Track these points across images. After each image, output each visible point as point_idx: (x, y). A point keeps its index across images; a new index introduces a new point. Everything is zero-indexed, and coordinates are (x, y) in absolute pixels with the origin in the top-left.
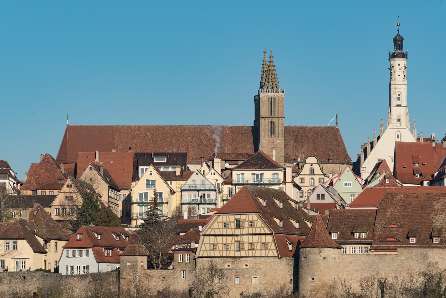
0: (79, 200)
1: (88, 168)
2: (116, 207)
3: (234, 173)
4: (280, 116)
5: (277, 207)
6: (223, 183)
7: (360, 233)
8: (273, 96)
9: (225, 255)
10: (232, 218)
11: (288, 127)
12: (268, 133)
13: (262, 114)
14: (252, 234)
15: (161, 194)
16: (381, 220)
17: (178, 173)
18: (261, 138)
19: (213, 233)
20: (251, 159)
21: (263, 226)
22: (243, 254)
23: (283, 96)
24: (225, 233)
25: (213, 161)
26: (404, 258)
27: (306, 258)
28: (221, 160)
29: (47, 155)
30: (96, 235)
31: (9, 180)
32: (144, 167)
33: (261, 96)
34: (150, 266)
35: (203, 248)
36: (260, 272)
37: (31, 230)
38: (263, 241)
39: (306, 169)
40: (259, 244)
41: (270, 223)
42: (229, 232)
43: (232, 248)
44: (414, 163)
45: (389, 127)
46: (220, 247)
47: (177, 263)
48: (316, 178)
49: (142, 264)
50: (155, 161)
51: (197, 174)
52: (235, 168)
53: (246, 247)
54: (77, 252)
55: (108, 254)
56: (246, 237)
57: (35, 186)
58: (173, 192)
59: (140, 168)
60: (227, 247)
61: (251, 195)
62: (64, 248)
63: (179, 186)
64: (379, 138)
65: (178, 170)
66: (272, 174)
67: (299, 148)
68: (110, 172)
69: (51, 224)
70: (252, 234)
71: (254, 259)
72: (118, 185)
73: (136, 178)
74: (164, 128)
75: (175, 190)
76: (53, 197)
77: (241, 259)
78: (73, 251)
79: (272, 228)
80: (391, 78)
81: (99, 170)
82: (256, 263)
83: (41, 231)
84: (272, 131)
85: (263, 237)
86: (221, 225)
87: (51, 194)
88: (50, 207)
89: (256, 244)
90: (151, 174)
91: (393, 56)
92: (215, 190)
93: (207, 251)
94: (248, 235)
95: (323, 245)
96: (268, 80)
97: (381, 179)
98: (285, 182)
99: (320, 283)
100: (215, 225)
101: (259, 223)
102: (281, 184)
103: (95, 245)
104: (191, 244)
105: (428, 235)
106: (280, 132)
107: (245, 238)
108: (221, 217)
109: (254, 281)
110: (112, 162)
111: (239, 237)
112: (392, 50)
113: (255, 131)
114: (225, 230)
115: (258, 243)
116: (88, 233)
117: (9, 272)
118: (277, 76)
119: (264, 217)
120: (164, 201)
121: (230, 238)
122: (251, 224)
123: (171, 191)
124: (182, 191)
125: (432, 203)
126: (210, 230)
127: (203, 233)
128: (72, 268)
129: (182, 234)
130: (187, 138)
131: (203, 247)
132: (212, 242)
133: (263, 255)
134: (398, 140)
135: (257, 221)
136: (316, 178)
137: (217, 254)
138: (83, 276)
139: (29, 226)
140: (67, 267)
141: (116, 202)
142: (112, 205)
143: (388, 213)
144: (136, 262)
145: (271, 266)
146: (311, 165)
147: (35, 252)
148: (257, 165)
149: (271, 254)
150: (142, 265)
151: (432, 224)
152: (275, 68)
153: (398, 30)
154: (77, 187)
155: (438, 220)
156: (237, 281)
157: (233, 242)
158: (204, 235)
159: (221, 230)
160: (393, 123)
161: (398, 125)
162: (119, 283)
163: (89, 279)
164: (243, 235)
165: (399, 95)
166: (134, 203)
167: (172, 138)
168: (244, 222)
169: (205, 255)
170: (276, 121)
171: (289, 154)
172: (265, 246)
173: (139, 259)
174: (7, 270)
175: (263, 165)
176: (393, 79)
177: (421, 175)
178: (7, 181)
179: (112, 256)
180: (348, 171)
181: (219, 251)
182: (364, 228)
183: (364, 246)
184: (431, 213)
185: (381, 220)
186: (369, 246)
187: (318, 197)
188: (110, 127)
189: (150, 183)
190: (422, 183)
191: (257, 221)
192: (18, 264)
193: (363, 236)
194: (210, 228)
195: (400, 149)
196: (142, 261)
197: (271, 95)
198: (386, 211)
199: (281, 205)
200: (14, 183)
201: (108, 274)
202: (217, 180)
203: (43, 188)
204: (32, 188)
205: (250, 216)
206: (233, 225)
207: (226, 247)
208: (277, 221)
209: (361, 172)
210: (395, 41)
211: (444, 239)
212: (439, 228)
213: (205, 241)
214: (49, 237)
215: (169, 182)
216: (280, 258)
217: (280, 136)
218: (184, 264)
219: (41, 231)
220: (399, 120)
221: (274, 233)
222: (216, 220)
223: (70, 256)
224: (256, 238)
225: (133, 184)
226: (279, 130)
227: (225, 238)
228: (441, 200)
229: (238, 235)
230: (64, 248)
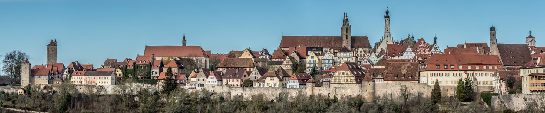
10: (341, 72)
39: (359, 52)
41: (353, 73)
76: (283, 62)
151: (401, 72)
189: (312, 57)
203: (278, 58)
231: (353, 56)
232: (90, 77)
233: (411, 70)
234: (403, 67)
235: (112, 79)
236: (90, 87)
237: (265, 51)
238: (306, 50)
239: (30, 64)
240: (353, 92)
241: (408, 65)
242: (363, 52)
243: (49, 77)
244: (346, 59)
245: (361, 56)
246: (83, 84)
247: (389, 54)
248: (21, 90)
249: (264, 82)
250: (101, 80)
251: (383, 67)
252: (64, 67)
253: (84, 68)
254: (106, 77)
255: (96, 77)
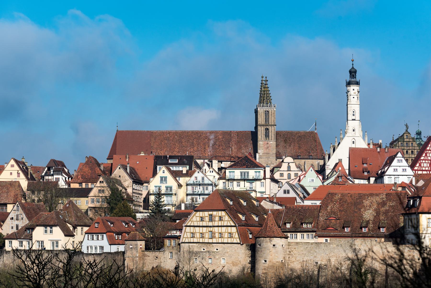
0: (107, 193)
1: (118, 168)
2: (140, 196)
3: (227, 171)
4: (273, 124)
5: (241, 205)
6: (219, 179)
7: (308, 223)
8: (267, 110)
9: (201, 241)
10: (206, 214)
11: (279, 132)
12: (264, 136)
13: (259, 123)
14: (221, 226)
15: (171, 188)
16: (323, 213)
17: (184, 172)
18: (258, 140)
19: (192, 224)
20: (240, 161)
21: (229, 220)
22: (214, 240)
23: (275, 109)
24: (201, 225)
25: (212, 162)
26: (335, 246)
27: (260, 245)
28: (218, 162)
29: (90, 157)
30: (109, 223)
31: (62, 175)
32: (161, 166)
33: (258, 109)
34: (148, 248)
35: (185, 236)
36: (227, 255)
37: (64, 218)
38: (229, 231)
39: (284, 167)
40: (226, 234)
42: (204, 224)
43: (207, 236)
44: (363, 164)
45: (347, 135)
46: (198, 235)
47: (166, 247)
48: (292, 174)
49: (141, 246)
50: (170, 162)
51: (198, 172)
52: (228, 167)
53: (217, 235)
54: (95, 237)
55: (118, 238)
56: (217, 228)
57: (81, 180)
58: (180, 186)
59: (158, 167)
60: (203, 235)
61: (221, 196)
62: (86, 233)
63: (185, 181)
64: (339, 143)
65: (184, 169)
66: (255, 172)
67: (288, 147)
68: (136, 170)
69: (79, 214)
70: (221, 226)
71: (223, 245)
72: (142, 180)
73: (155, 173)
74: (188, 132)
75: (182, 184)
76: (91, 189)
77: (213, 244)
78: (92, 236)
79: (236, 221)
80: (348, 100)
81: (125, 169)
82: (224, 248)
83: (71, 220)
84: (267, 135)
85: (229, 228)
86: (198, 219)
87: (93, 186)
88: (88, 197)
89: (224, 234)
90: (164, 172)
91: (349, 84)
92: (211, 185)
93: (188, 238)
94: (218, 226)
95: (273, 236)
96: (265, 97)
97: (336, 176)
98: (265, 178)
99: (271, 264)
100: (194, 219)
101: (227, 218)
102: (261, 180)
103: (108, 231)
104: (181, 230)
105: (359, 226)
106: (273, 136)
107: (216, 229)
108: (198, 212)
109: (223, 262)
110: (138, 163)
111: (211, 228)
112: (348, 79)
113: (254, 135)
114: (201, 222)
115: (225, 232)
116: (103, 222)
117: (46, 250)
118: (271, 95)
119: (230, 213)
120: (174, 192)
121: (205, 229)
122: (221, 218)
123: (178, 185)
124: (187, 185)
125: (362, 201)
126: (190, 222)
127: (185, 225)
128: (91, 247)
129: (177, 221)
130: (204, 140)
131: (186, 234)
132: (192, 231)
133: (229, 242)
134: (353, 146)
135: (225, 216)
136: (292, 174)
137: (195, 240)
138: (99, 254)
139: (62, 216)
140: (88, 247)
141: (140, 192)
142: (136, 195)
143: (329, 208)
144: (137, 245)
145: (235, 251)
146: (289, 164)
147: (66, 235)
148: (244, 165)
149: (235, 241)
150: (141, 248)
151: (362, 217)
152: (269, 89)
153: (353, 64)
154: (107, 182)
155: (367, 214)
156: (210, 261)
157: (207, 231)
158: (186, 226)
159: (198, 222)
160: (350, 132)
161: (353, 134)
162: (124, 260)
163: (103, 256)
164: (214, 226)
165: (354, 112)
166: (151, 194)
167: (193, 140)
168: (215, 217)
169: (187, 241)
170: (270, 128)
171: (280, 152)
172: (231, 235)
173: (139, 243)
174: (45, 249)
175: (249, 165)
176: (349, 100)
177: (368, 172)
178: (60, 177)
179: (121, 240)
180: (311, 171)
181: (197, 238)
182: (311, 220)
183: (310, 234)
184: (361, 208)
185: (323, 213)
186: (314, 234)
187: (285, 192)
188: (148, 132)
189: (163, 179)
190: (369, 179)
191: (225, 216)
192: (53, 243)
193: (309, 226)
194: (190, 221)
195: (353, 152)
196: (142, 244)
197: (266, 109)
198: (328, 207)
199: (245, 204)
200: (66, 178)
201: (117, 253)
202: (214, 177)
203: (87, 182)
204: (79, 181)
205: (220, 212)
206: (207, 219)
207: (202, 235)
208: (240, 216)
209: (326, 168)
210: (350, 72)
211: (371, 228)
212: (367, 220)
213: (187, 231)
214: (77, 224)
215: (178, 178)
216: (242, 245)
217: (273, 139)
218: (171, 247)
219: (71, 220)
220: (354, 130)
221: (237, 225)
222: (195, 215)
223: (90, 239)
224: (224, 229)
225: (151, 179)
226: (272, 134)
227: (201, 228)
228: (369, 198)
229: (210, 227)
230: (86, 233)
231: (265, 178)
233: (386, 213)
234: (366, 203)
237: (57, 166)
238: (151, 162)
240: (234, 264)
241: (378, 199)
242: (293, 167)
244: (248, 185)
245: (289, 176)
247: (353, 174)
249: (30, 238)
251: (318, 203)
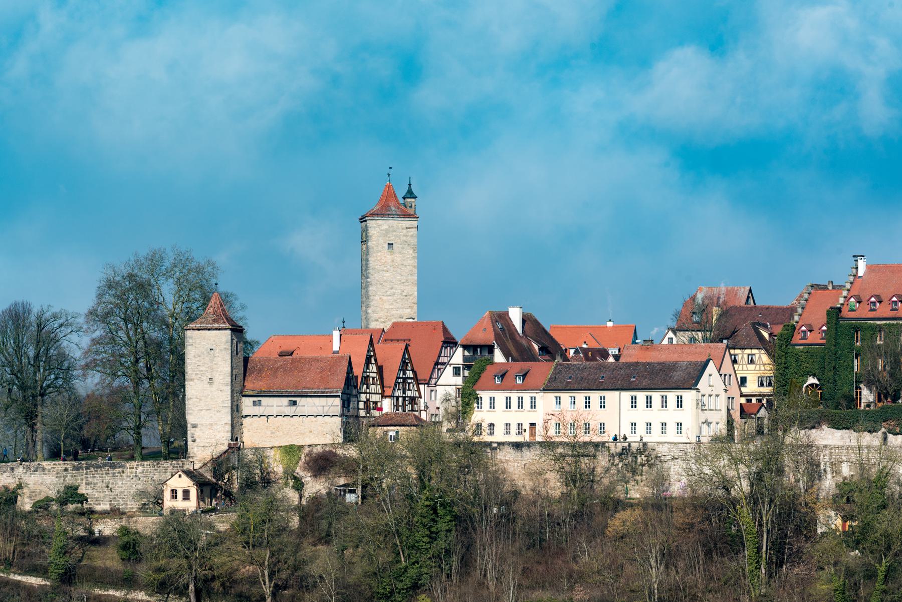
232: (580, 396)
235: (701, 405)
236: (575, 454)
239: (237, 331)
243: (345, 404)
246: (539, 439)
248: (182, 483)
250: (641, 415)
252: (450, 342)
253: (571, 344)
254: (672, 395)
255: (612, 397)
